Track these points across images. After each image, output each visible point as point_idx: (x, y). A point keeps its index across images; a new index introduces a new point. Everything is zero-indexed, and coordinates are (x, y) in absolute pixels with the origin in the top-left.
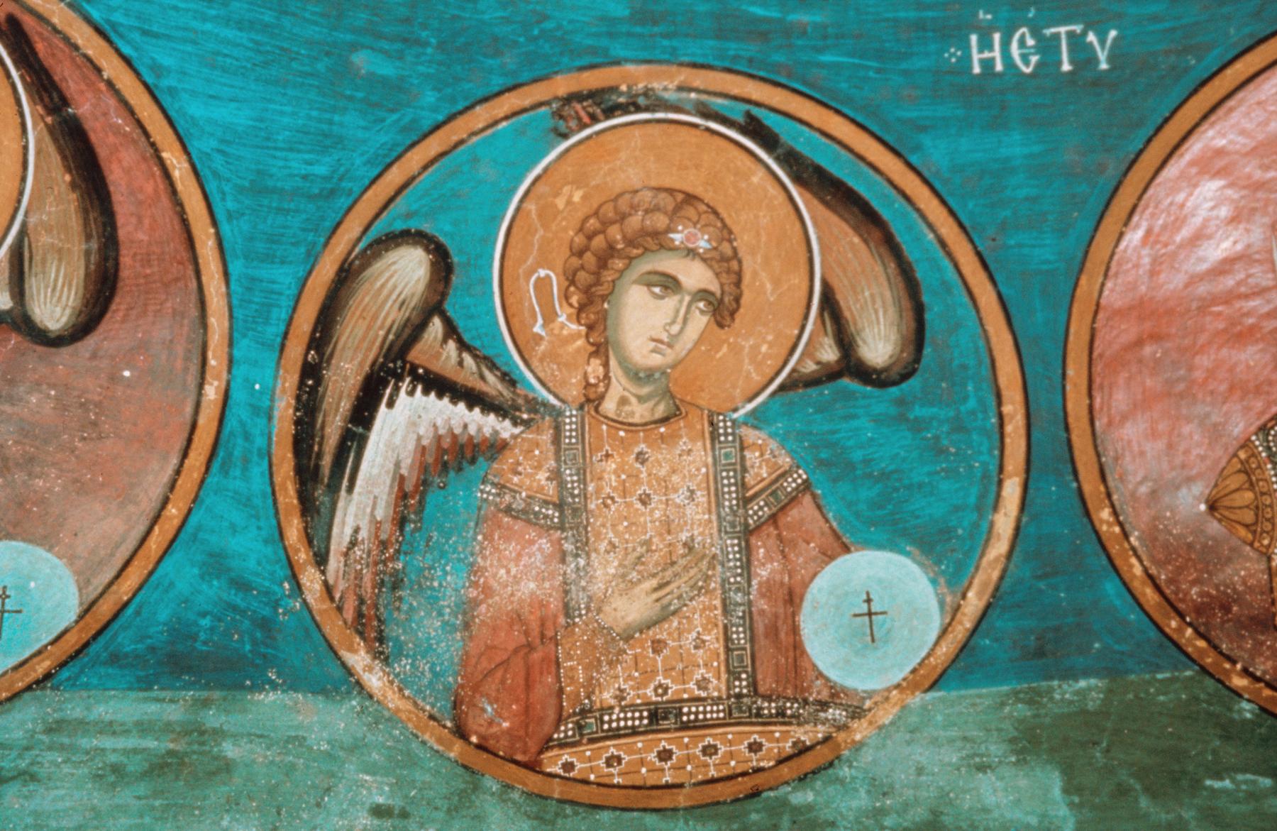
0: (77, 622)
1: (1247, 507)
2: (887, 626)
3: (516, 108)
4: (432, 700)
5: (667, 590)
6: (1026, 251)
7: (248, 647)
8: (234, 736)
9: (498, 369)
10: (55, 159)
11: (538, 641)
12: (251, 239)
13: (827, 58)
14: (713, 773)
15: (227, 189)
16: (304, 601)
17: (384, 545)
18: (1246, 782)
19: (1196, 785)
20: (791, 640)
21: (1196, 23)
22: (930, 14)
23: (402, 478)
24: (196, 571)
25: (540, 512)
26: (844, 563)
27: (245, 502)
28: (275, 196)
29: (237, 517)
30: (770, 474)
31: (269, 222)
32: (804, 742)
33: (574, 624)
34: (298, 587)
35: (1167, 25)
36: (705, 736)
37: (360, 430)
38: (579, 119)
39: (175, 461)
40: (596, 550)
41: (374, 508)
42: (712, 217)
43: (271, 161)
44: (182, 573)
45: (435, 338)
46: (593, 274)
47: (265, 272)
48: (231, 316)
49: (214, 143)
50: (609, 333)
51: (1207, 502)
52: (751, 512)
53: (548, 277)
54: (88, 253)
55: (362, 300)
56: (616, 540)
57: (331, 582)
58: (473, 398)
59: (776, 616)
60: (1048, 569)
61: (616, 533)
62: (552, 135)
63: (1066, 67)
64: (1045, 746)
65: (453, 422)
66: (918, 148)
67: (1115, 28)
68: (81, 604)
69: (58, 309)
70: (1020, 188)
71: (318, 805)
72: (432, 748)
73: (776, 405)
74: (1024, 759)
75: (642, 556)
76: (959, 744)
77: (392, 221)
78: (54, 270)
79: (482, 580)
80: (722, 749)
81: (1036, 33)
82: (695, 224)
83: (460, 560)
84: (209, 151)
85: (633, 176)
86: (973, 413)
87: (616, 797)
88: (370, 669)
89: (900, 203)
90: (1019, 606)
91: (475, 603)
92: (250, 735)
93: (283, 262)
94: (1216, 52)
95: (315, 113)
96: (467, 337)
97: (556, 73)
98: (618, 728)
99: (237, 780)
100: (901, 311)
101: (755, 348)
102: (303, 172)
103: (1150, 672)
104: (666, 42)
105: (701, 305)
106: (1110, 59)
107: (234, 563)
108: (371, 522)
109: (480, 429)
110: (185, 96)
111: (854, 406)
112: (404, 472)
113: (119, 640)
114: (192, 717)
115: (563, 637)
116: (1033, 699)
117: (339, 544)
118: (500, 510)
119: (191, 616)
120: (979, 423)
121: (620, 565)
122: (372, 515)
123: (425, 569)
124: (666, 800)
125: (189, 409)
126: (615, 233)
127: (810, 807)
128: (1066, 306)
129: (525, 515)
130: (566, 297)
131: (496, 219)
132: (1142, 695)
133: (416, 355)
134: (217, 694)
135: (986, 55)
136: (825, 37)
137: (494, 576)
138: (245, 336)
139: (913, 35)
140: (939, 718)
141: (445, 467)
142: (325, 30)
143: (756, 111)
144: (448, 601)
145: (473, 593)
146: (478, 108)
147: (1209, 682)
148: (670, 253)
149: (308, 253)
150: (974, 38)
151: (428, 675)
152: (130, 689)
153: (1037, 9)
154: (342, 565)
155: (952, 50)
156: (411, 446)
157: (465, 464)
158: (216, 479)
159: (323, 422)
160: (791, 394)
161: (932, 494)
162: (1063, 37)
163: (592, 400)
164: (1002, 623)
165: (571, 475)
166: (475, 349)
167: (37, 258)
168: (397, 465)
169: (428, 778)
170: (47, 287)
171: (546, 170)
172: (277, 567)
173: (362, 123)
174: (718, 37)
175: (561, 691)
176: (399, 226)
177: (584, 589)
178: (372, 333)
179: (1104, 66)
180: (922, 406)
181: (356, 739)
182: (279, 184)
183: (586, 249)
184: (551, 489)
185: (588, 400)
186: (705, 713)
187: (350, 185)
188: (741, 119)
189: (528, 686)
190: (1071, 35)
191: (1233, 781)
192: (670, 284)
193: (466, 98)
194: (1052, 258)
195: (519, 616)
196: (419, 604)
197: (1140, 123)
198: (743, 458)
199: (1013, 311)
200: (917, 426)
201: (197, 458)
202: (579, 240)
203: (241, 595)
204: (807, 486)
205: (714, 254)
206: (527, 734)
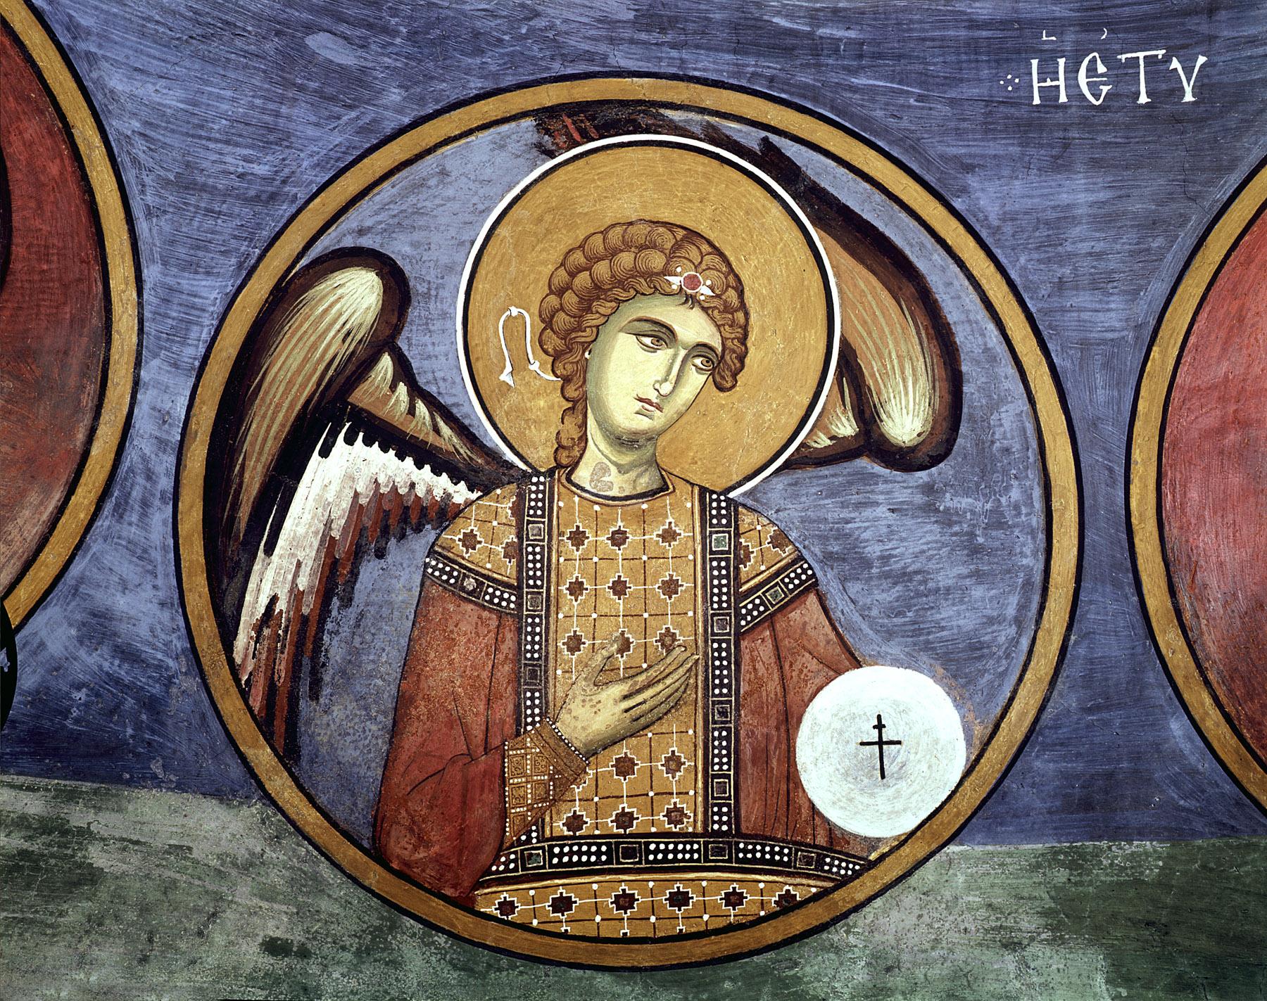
2: (899, 760)
6: (1085, 316)
7: (130, 731)
8: (103, 839)
12: (172, 242)
14: (681, 927)
15: (148, 180)
22: (984, 34)
24: (73, 632)
27: (141, 554)
28: (205, 195)
29: (128, 569)
31: (196, 224)
38: (569, 135)
39: (57, 496)
41: (296, 575)
42: (717, 259)
43: (202, 153)
47: (186, 282)
48: (141, 330)
49: (136, 125)
50: (590, 387)
52: (744, 611)
55: (301, 326)
58: (423, 454)
59: (768, 737)
62: (535, 152)
63: (1143, 99)
65: (397, 480)
66: (964, 190)
70: (1081, 240)
74: (1061, 937)
76: (983, 913)
84: (129, 133)
85: (627, 206)
86: (1016, 507)
87: (563, 950)
89: (939, 256)
90: (1062, 744)
92: (124, 840)
93: (208, 273)
95: (258, 102)
96: (421, 381)
99: (103, 895)
101: (759, 415)
102: (240, 170)
104: (674, 53)
105: (698, 361)
107: (123, 628)
108: (291, 591)
109: (429, 491)
111: (872, 492)
112: (336, 534)
114: (54, 813)
116: (1077, 862)
124: (625, 957)
125: (81, 436)
126: (602, 269)
128: (1133, 382)
132: (1212, 865)
133: (362, 397)
134: (86, 786)
136: (861, 57)
138: (156, 356)
139: (964, 57)
141: (385, 532)
142: (277, 6)
143: (774, 139)
148: (666, 299)
149: (240, 266)
156: (346, 504)
157: (409, 532)
158: (107, 523)
159: (243, 466)
160: (799, 474)
161: (962, 601)
162: (1142, 62)
164: (1041, 764)
168: (328, 524)
169: (336, 909)
173: (313, 119)
174: (735, 52)
175: (504, 814)
176: (348, 242)
179: (1189, 97)
180: (955, 494)
181: (252, 854)
182: (211, 181)
183: (569, 287)
184: (509, 570)
185: (559, 466)
186: (675, 851)
187: (295, 190)
189: (465, 804)
192: (662, 335)
193: (437, 101)
194: (1118, 325)
197: (1231, 168)
198: (738, 545)
199: (1068, 385)
200: (948, 519)
203: (126, 666)
205: (716, 303)
206: (459, 863)
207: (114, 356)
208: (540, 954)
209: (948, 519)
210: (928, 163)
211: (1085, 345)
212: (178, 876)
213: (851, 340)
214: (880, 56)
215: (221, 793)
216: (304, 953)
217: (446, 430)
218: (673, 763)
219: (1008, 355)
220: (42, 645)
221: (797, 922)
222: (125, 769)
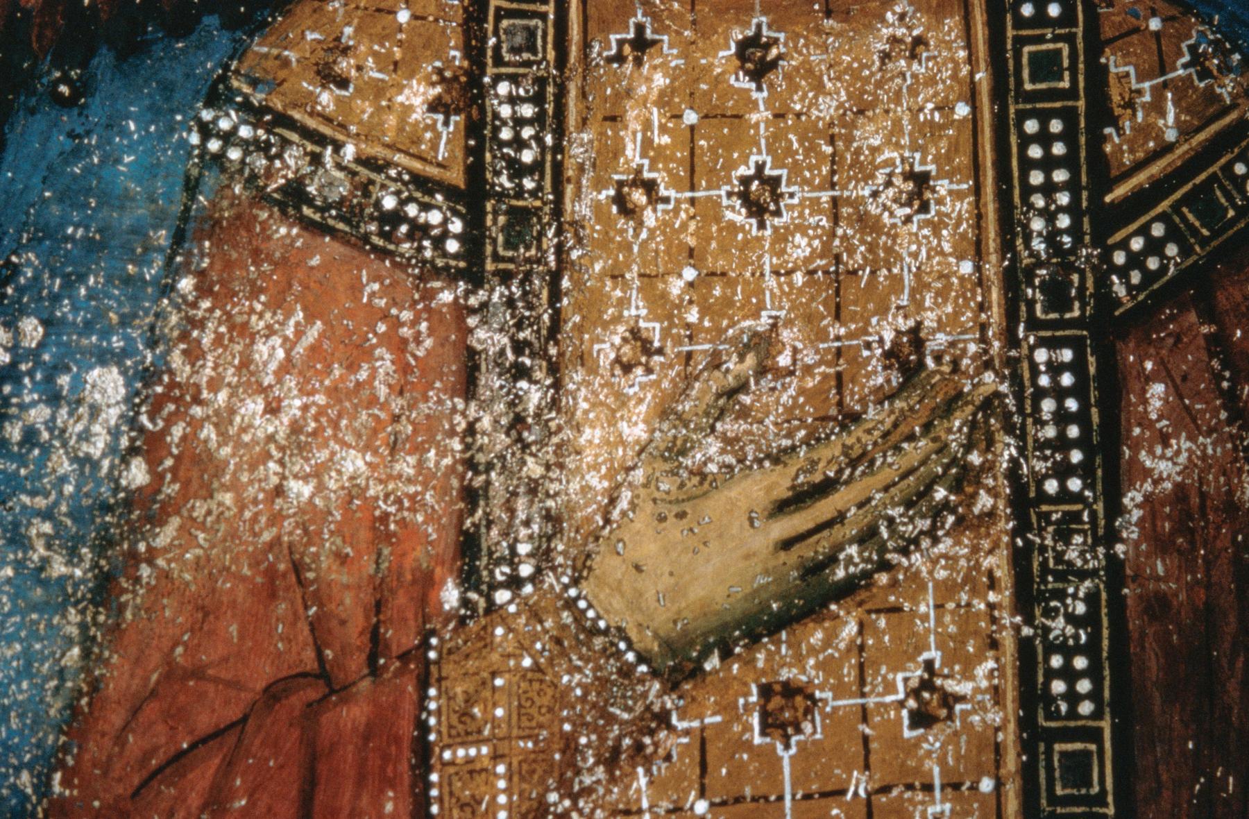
5: (824, 509)
11: (356, 663)
25: (396, 217)
30: (1186, 132)
33: (491, 608)
40: (583, 359)
52: (1119, 258)
56: (654, 330)
59: (1209, 614)
61: (662, 306)
75: (743, 387)
79: (178, 431)
91: (145, 508)
115: (447, 653)
118: (262, 198)
121: (664, 411)
129: (355, 225)
137: (223, 420)
165: (513, 100)
177: (533, 488)
184: (445, 140)
195: (298, 568)
198: (1098, 76)
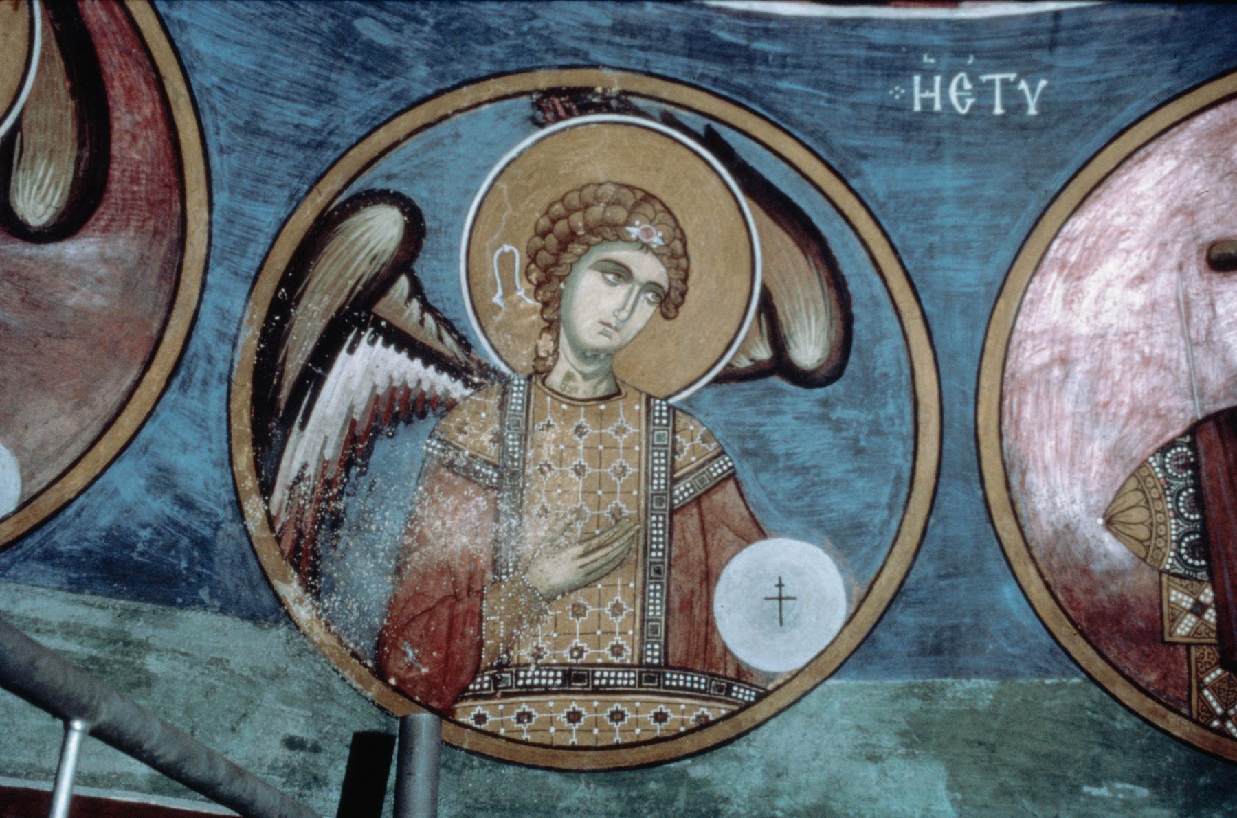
0: (14, 513)
1: (1142, 523)
3: (500, 94)
4: (357, 638)
6: (950, 274)
7: (184, 564)
8: (158, 650)
9: (456, 332)
10: (59, 64)
11: (464, 593)
12: (239, 175)
13: (783, 85)
14: (618, 739)
15: (222, 124)
16: (245, 527)
17: (329, 484)
18: (1123, 791)
19: (1075, 789)
20: (704, 616)
21: (1119, 77)
23: (353, 424)
24: (142, 482)
25: (480, 471)
26: (759, 550)
27: (200, 423)
29: (191, 435)
31: (258, 162)
32: (707, 717)
34: (240, 514)
35: (1094, 77)
36: (615, 701)
37: (320, 371)
38: (556, 112)
40: (528, 513)
41: (323, 447)
42: (667, 217)
44: (128, 481)
45: (401, 296)
46: (554, 255)
47: (249, 208)
48: (209, 245)
49: (215, 79)
50: (563, 312)
51: (1104, 516)
53: (512, 253)
54: (78, 160)
55: (337, 248)
56: (549, 506)
57: (274, 513)
58: (430, 356)
59: (692, 592)
60: (951, 570)
61: (550, 500)
62: (529, 123)
63: (998, 110)
64: (934, 741)
66: (859, 174)
67: (1046, 78)
68: (22, 496)
69: (41, 208)
70: (948, 216)
71: (233, 730)
72: (350, 685)
73: (710, 394)
74: (913, 753)
76: (853, 733)
77: (373, 180)
78: (42, 169)
79: (418, 529)
80: (629, 716)
81: (973, 78)
82: (651, 222)
83: (400, 508)
85: (598, 170)
86: (891, 419)
87: (524, 753)
88: (301, 601)
89: (839, 223)
90: (920, 602)
91: (408, 550)
92: (175, 651)
93: (266, 202)
94: (1136, 104)
96: (430, 299)
97: (540, 67)
98: (532, 686)
100: (831, 320)
102: (296, 122)
103: (1039, 676)
104: (641, 54)
105: (650, 295)
106: (1041, 104)
107: (182, 481)
108: (319, 460)
109: (432, 387)
110: (194, 31)
112: (357, 417)
113: (56, 538)
115: (489, 592)
116: (928, 695)
117: (287, 477)
118: (443, 465)
119: (133, 527)
120: (896, 428)
121: (550, 529)
122: (321, 453)
123: (365, 512)
124: (571, 762)
126: (577, 220)
127: (706, 782)
129: (469, 475)
130: (527, 273)
131: (470, 193)
132: (1030, 699)
133: (382, 308)
134: (148, 607)
135: (927, 95)
136: (784, 66)
137: (430, 526)
138: (220, 264)
140: (837, 705)
143: (716, 126)
144: (385, 544)
145: (408, 540)
146: (465, 89)
147: (1096, 691)
148: (627, 245)
149: (291, 197)
150: (917, 79)
151: (356, 614)
152: (60, 589)
153: (976, 57)
154: (286, 497)
155: (897, 88)
156: (366, 393)
157: (415, 418)
158: (174, 396)
160: (725, 387)
163: (539, 372)
164: (905, 618)
165: (513, 440)
166: (437, 311)
167: (28, 154)
168: (351, 408)
169: (343, 714)
170: (32, 184)
171: (521, 154)
172: (223, 491)
174: (689, 56)
175: (481, 644)
176: (379, 185)
177: (513, 548)
178: (341, 282)
179: (1032, 111)
180: (844, 407)
181: (278, 668)
182: (272, 129)
183: (550, 231)
184: (492, 450)
185: (537, 372)
186: (616, 678)
188: (702, 132)
189: (450, 637)
190: (1005, 83)
191: (1110, 788)
192: (622, 273)
193: (454, 78)
195: (449, 567)
196: (357, 545)
197: (1063, 164)
198: (674, 441)
200: (838, 427)
201: (158, 373)
202: (545, 223)
203: (184, 512)
204: (732, 476)
206: (444, 682)
207: (187, 262)
208: (503, 754)
209: (838, 427)
210: (831, 151)
211: (948, 296)
212: (216, 683)
213: (769, 285)
214: (799, 66)
215: (254, 616)
216: (316, 749)
217: (448, 340)
218: (617, 609)
219: (888, 301)
220: (116, 492)
221: (709, 737)
222: (178, 594)
